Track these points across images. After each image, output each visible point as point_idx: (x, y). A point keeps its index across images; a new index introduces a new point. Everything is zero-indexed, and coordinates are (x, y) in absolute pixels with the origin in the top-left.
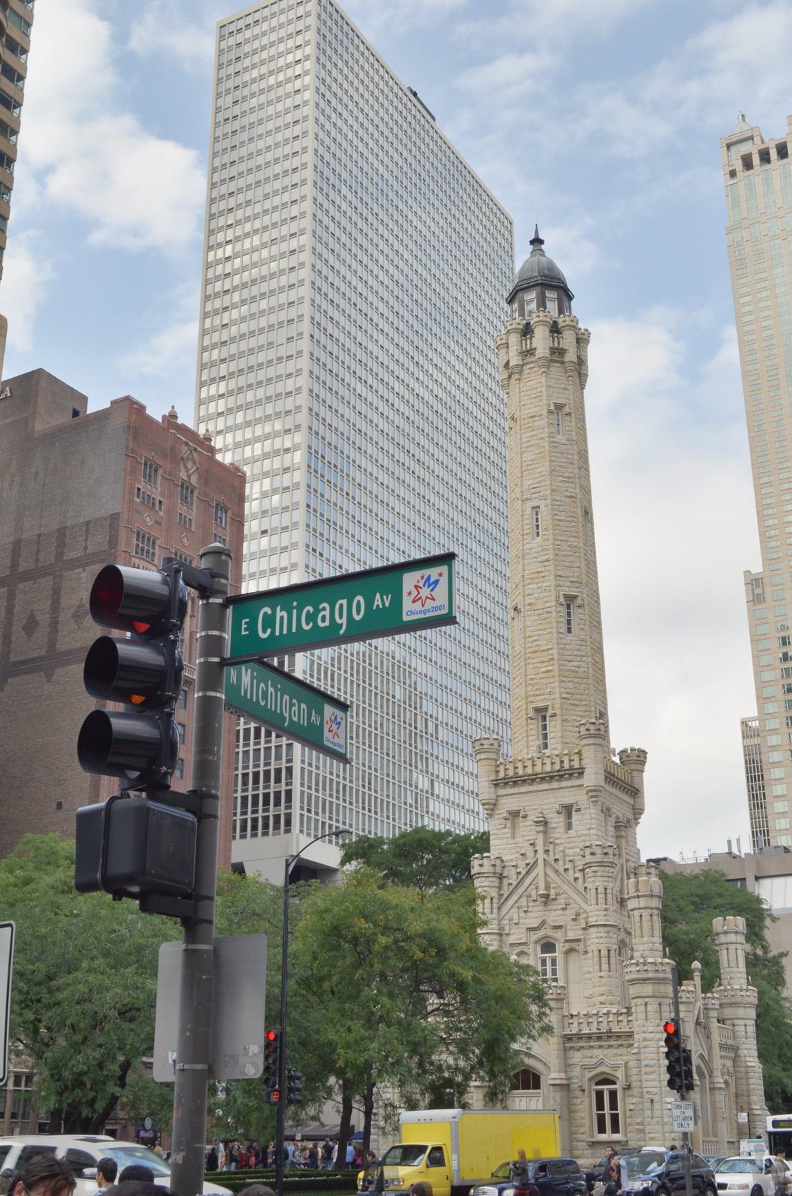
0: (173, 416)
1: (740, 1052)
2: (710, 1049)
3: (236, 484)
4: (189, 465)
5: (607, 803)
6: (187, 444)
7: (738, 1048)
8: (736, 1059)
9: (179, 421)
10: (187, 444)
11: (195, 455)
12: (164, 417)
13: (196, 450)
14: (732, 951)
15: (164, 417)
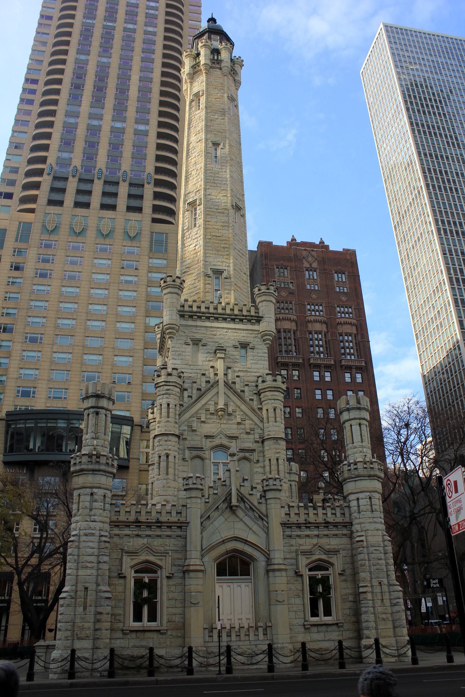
0: (293, 239)
1: (356, 527)
2: (267, 531)
3: (348, 258)
4: (310, 259)
5: (198, 336)
6: (306, 250)
7: (351, 524)
8: (351, 536)
9: (298, 241)
10: (306, 250)
11: (313, 253)
12: (287, 242)
13: (313, 251)
14: (356, 428)
15: (287, 242)
